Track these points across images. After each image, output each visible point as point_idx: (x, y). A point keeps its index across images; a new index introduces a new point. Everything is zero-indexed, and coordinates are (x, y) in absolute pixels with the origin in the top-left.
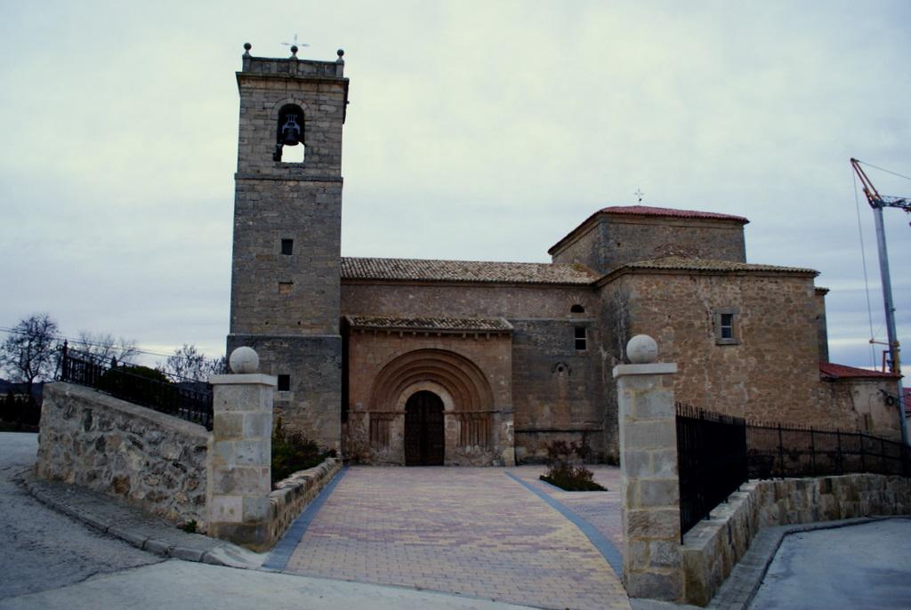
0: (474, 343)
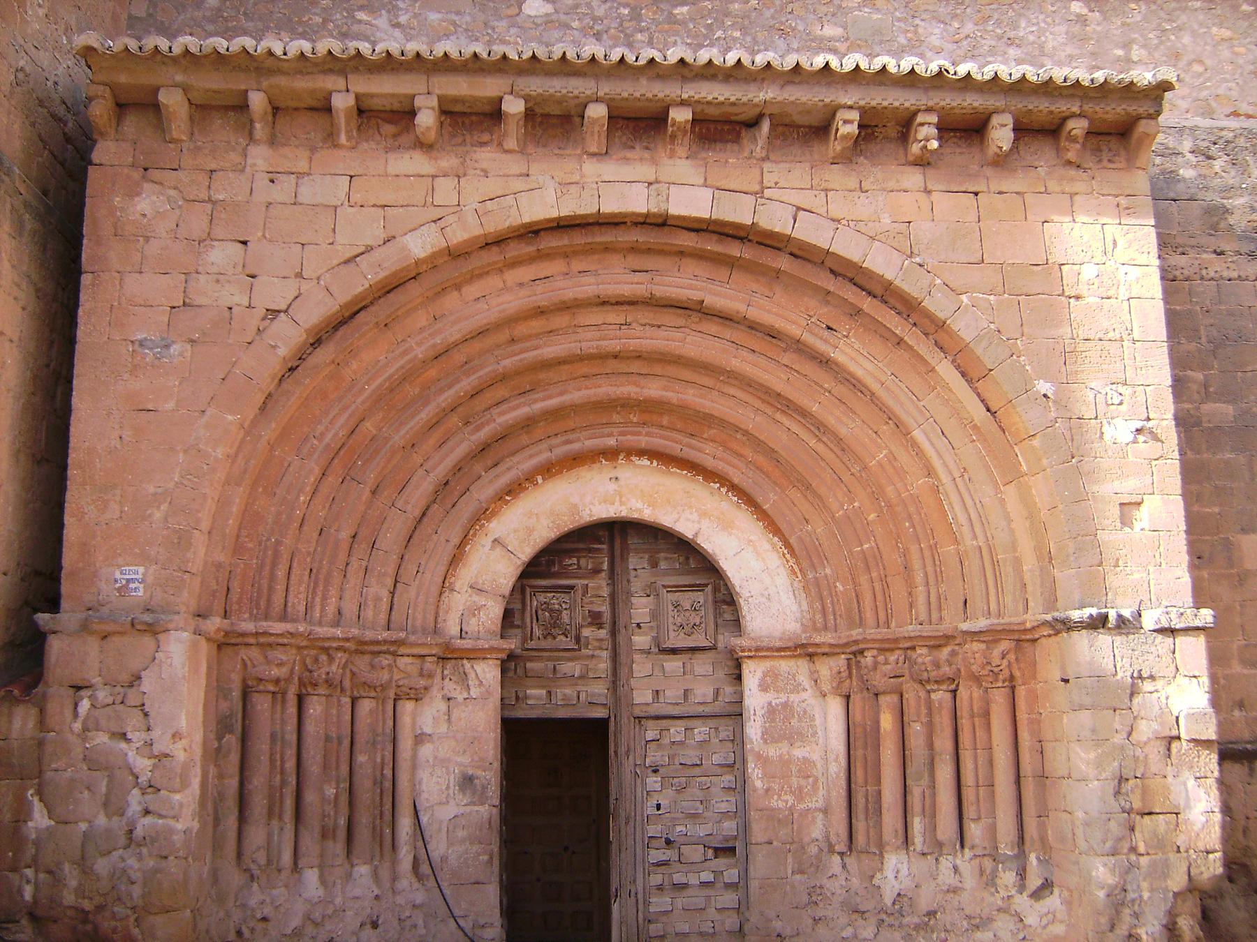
0: (913, 178)
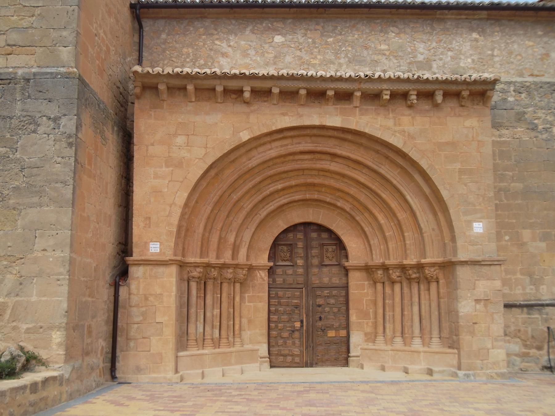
0: (407, 111)
